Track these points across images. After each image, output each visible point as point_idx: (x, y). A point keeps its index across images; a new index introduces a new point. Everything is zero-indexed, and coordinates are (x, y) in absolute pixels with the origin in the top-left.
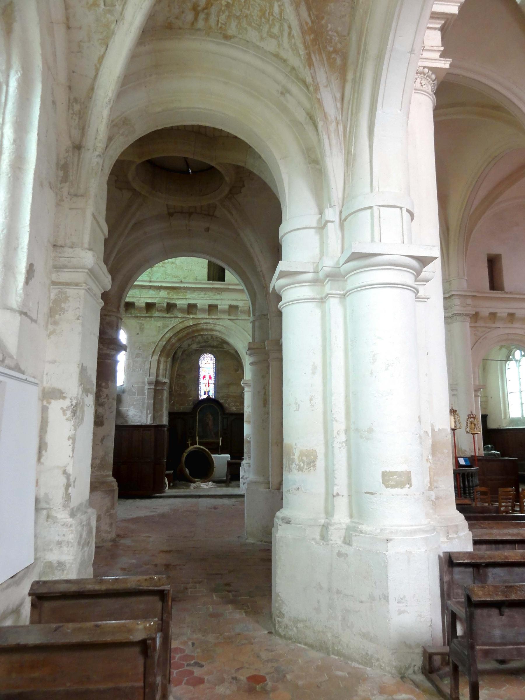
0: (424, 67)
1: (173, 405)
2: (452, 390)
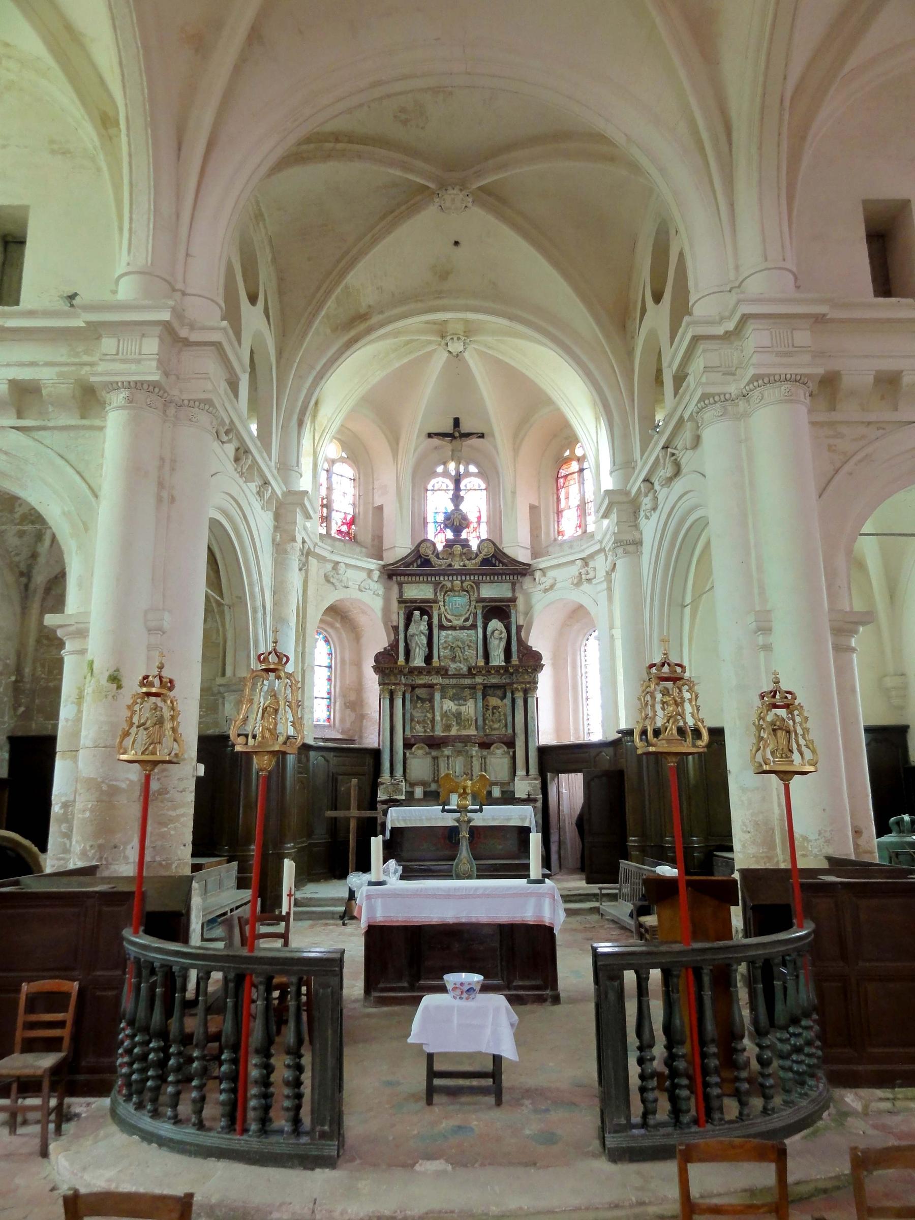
1: (27, 716)
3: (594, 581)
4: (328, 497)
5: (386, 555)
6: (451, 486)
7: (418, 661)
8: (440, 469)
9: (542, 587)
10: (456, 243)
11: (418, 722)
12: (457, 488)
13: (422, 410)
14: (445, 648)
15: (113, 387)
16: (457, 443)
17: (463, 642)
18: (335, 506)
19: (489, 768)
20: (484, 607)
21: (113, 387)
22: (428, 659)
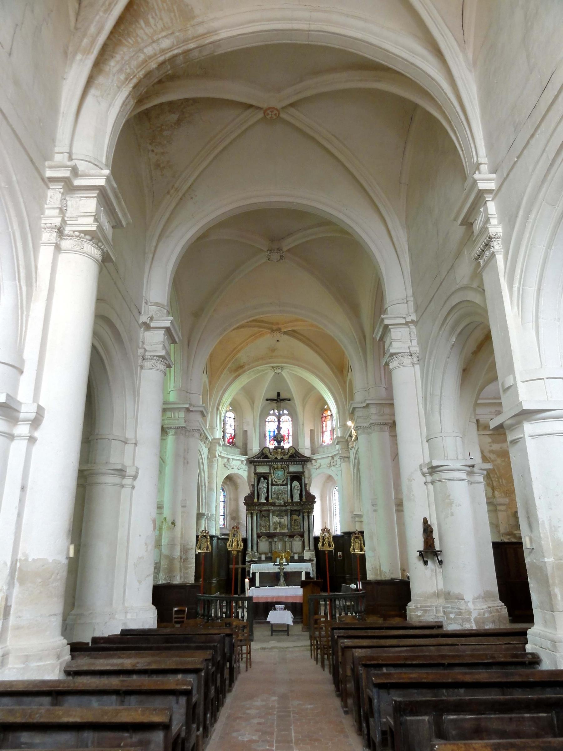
0: (74, 232)
2: (373, 505)
3: (336, 466)
4: (224, 428)
5: (249, 452)
6: (276, 420)
7: (263, 500)
8: (272, 412)
9: (315, 467)
10: (278, 341)
11: (263, 527)
12: (279, 421)
13: (264, 390)
14: (274, 494)
15: (171, 428)
16: (279, 403)
17: (282, 491)
18: (227, 431)
19: (294, 547)
20: (291, 476)
21: (171, 428)
22: (267, 499)
